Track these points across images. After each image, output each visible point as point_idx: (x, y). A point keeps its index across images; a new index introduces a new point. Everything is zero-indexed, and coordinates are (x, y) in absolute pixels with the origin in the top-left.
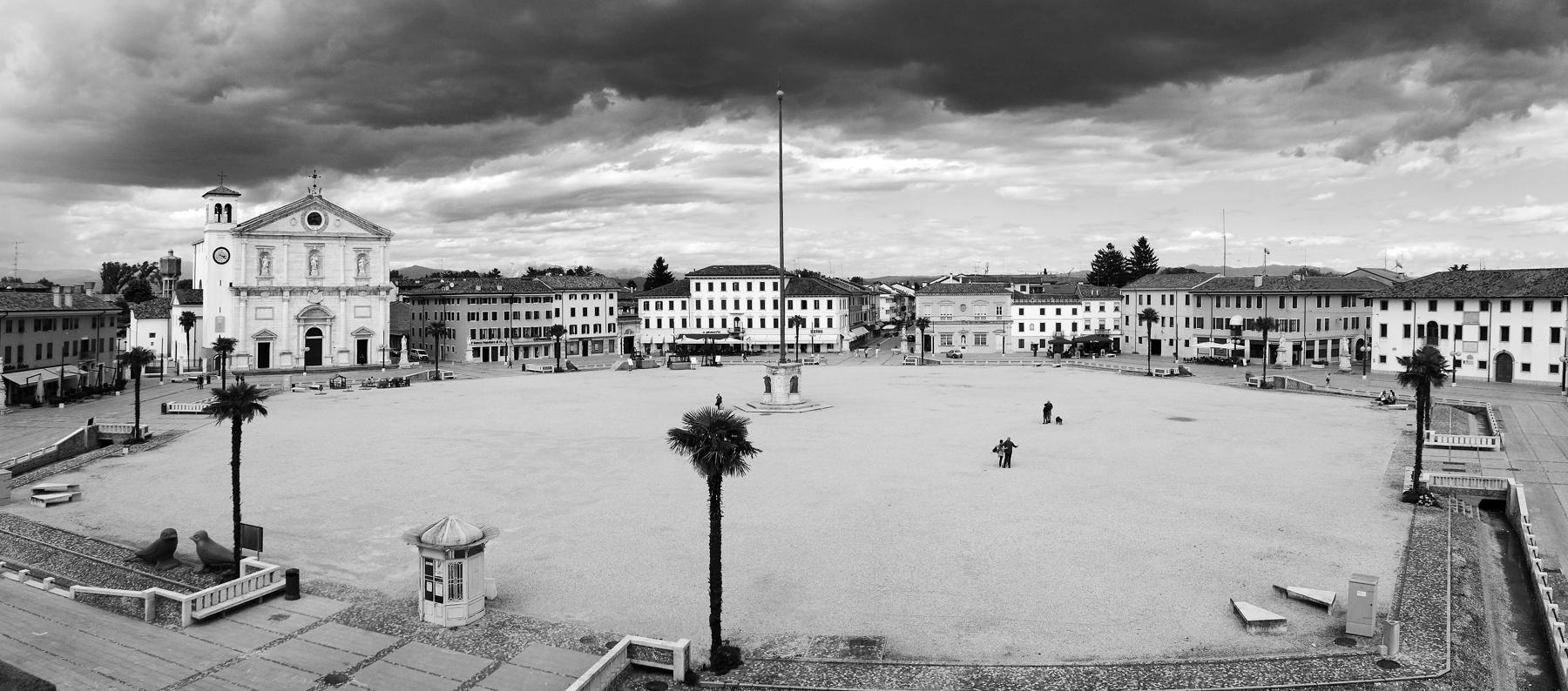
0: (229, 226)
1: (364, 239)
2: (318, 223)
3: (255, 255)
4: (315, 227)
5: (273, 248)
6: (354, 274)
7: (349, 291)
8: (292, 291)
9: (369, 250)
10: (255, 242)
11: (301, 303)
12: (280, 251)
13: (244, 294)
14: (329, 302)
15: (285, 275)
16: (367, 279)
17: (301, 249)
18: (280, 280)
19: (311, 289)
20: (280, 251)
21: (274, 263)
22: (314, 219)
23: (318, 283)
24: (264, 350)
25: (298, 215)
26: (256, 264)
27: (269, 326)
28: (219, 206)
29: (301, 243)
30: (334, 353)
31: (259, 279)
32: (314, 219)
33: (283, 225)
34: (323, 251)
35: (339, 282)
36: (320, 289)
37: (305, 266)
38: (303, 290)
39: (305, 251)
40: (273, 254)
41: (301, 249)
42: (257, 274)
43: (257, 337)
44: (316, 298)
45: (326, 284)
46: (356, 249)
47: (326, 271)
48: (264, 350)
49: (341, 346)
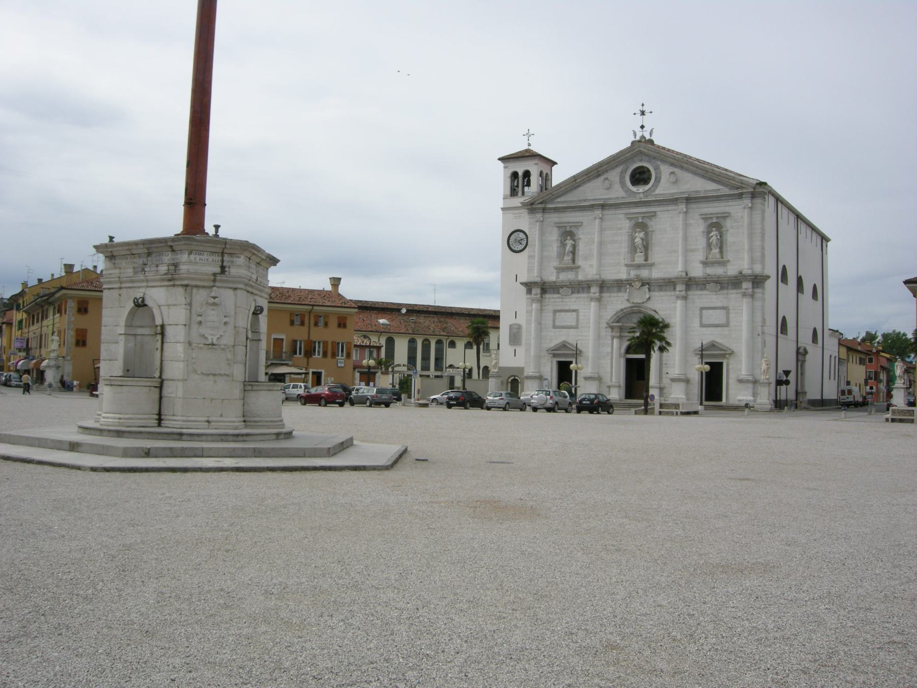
0: (522, 199)
1: (718, 198)
2: (646, 181)
3: (554, 236)
4: (641, 189)
5: (578, 225)
6: (700, 256)
7: (690, 283)
8: (603, 286)
9: (726, 216)
10: (554, 218)
11: (618, 302)
12: (590, 230)
13: (536, 291)
14: (665, 307)
15: (594, 262)
16: (723, 263)
17: (620, 225)
18: (588, 269)
19: (629, 283)
20: (590, 230)
21: (582, 249)
22: (640, 177)
23: (645, 273)
24: (565, 372)
25: (614, 175)
26: (554, 248)
27: (570, 337)
28: (515, 175)
29: (620, 214)
30: (666, 381)
31: (560, 270)
32: (640, 177)
33: (594, 191)
34: (653, 224)
35: (676, 269)
36: (646, 283)
37: (624, 248)
38: (620, 285)
39: (626, 225)
40: (581, 234)
41: (620, 225)
42: (555, 263)
43: (553, 352)
44: (639, 296)
45: (656, 274)
46: (705, 218)
47: (657, 255)
48: (565, 372)
49: (675, 371)
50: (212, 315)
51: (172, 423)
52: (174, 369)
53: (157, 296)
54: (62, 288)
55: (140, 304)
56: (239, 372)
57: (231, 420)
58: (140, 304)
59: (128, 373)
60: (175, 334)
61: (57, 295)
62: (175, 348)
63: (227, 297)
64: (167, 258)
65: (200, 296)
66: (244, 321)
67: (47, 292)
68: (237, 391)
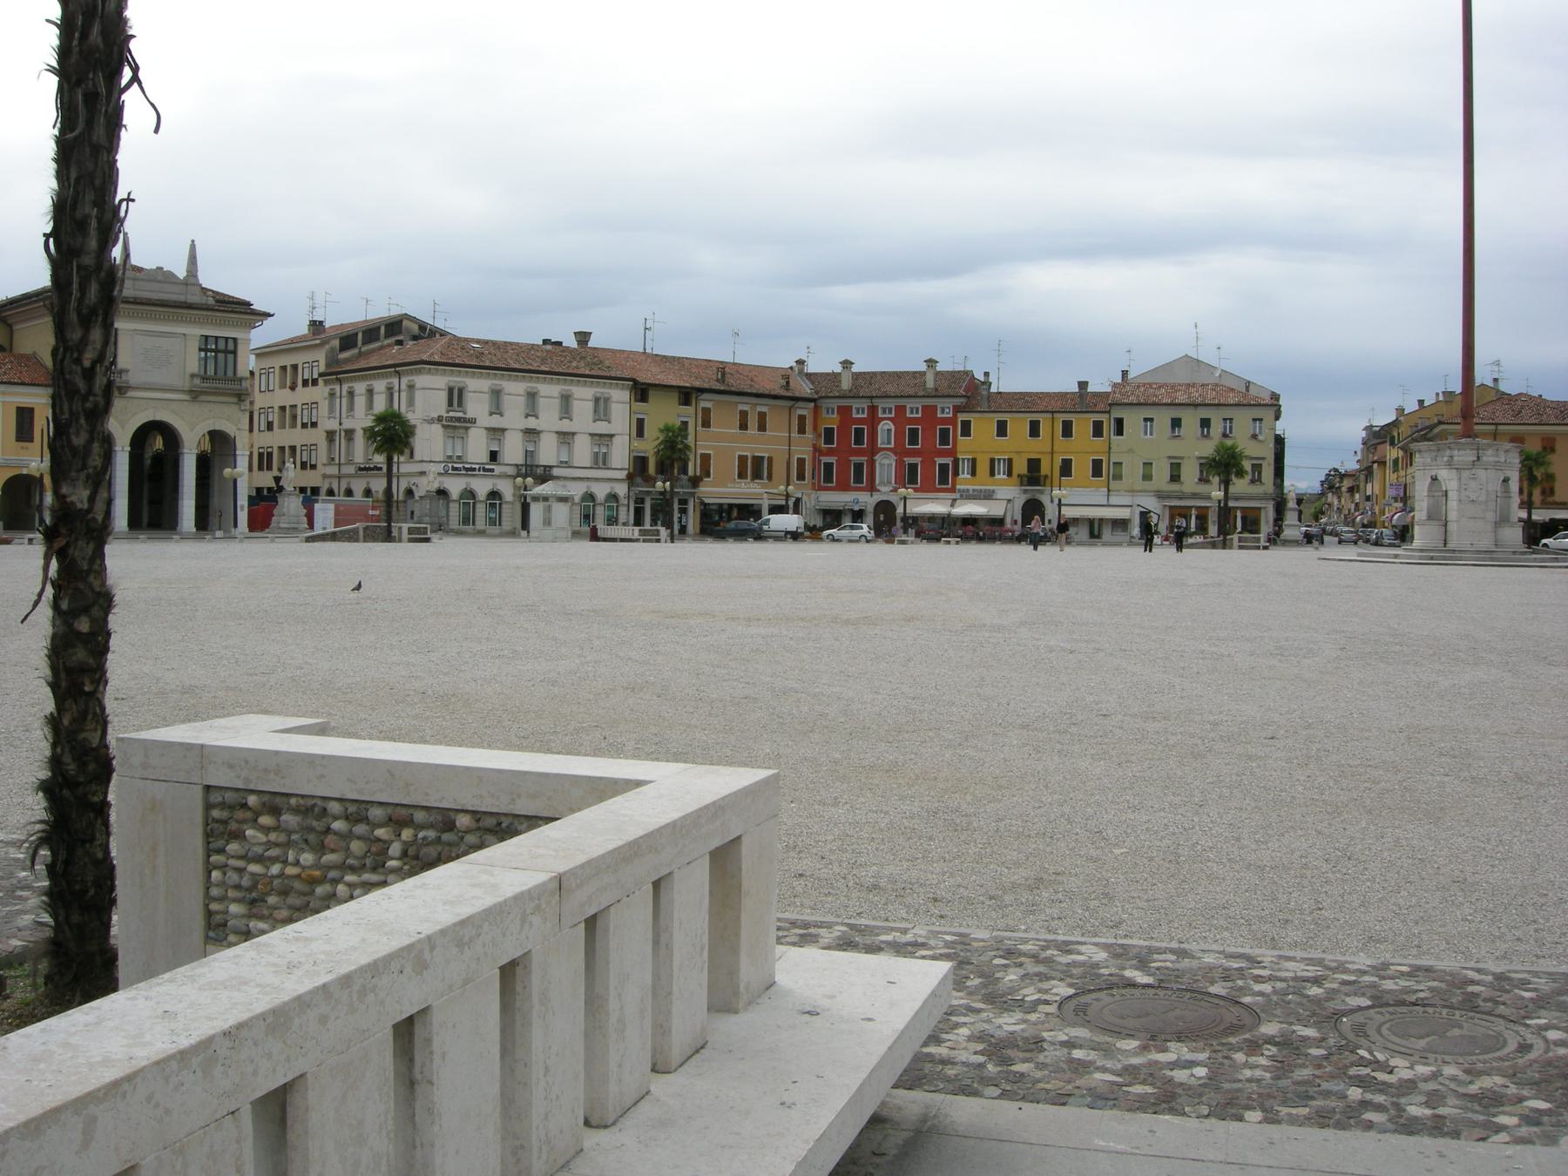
50: (1473, 484)
51: (1450, 546)
52: (1452, 515)
53: (1443, 474)
54: (1440, 423)
55: (1434, 479)
56: (1491, 516)
57: (1485, 543)
58: (1434, 479)
59: (1430, 518)
60: (1453, 495)
61: (1436, 431)
62: (1453, 504)
63: (1482, 474)
64: (1448, 452)
65: (1466, 474)
66: (1496, 486)
67: (1428, 423)
68: (1489, 527)
